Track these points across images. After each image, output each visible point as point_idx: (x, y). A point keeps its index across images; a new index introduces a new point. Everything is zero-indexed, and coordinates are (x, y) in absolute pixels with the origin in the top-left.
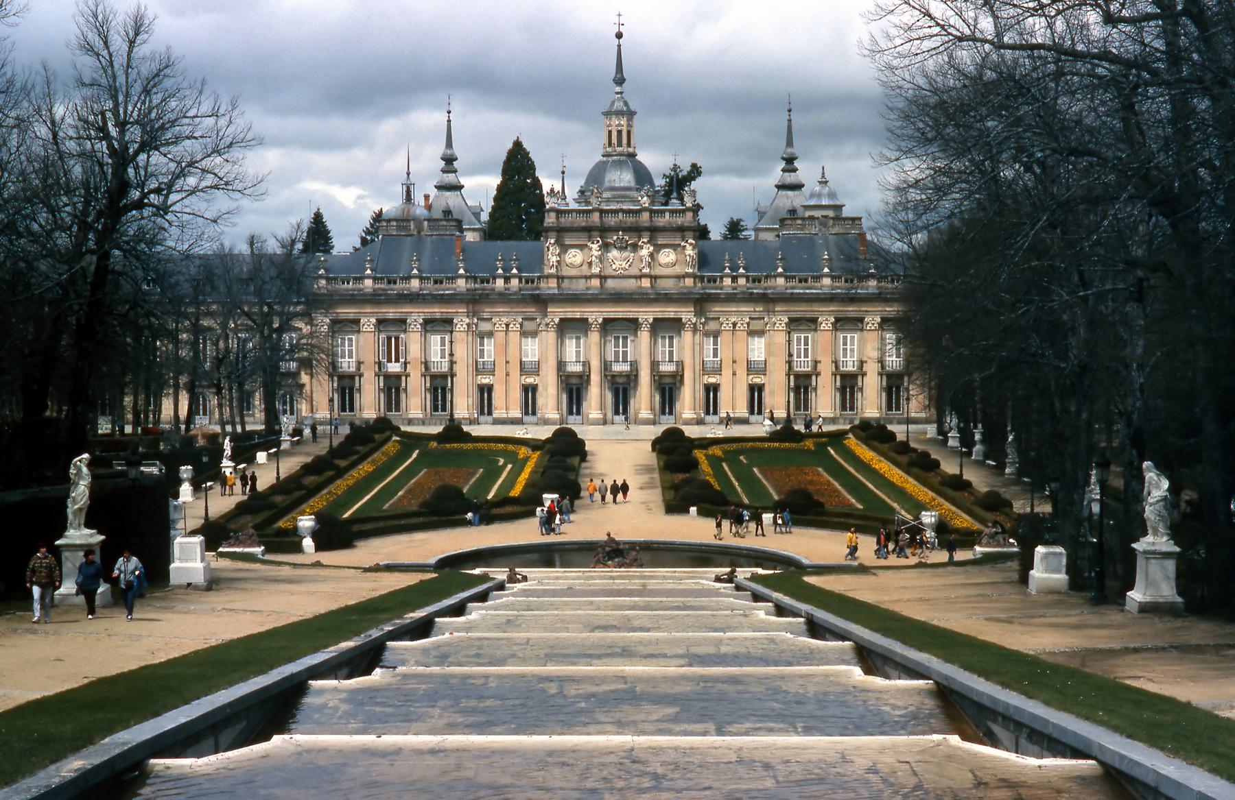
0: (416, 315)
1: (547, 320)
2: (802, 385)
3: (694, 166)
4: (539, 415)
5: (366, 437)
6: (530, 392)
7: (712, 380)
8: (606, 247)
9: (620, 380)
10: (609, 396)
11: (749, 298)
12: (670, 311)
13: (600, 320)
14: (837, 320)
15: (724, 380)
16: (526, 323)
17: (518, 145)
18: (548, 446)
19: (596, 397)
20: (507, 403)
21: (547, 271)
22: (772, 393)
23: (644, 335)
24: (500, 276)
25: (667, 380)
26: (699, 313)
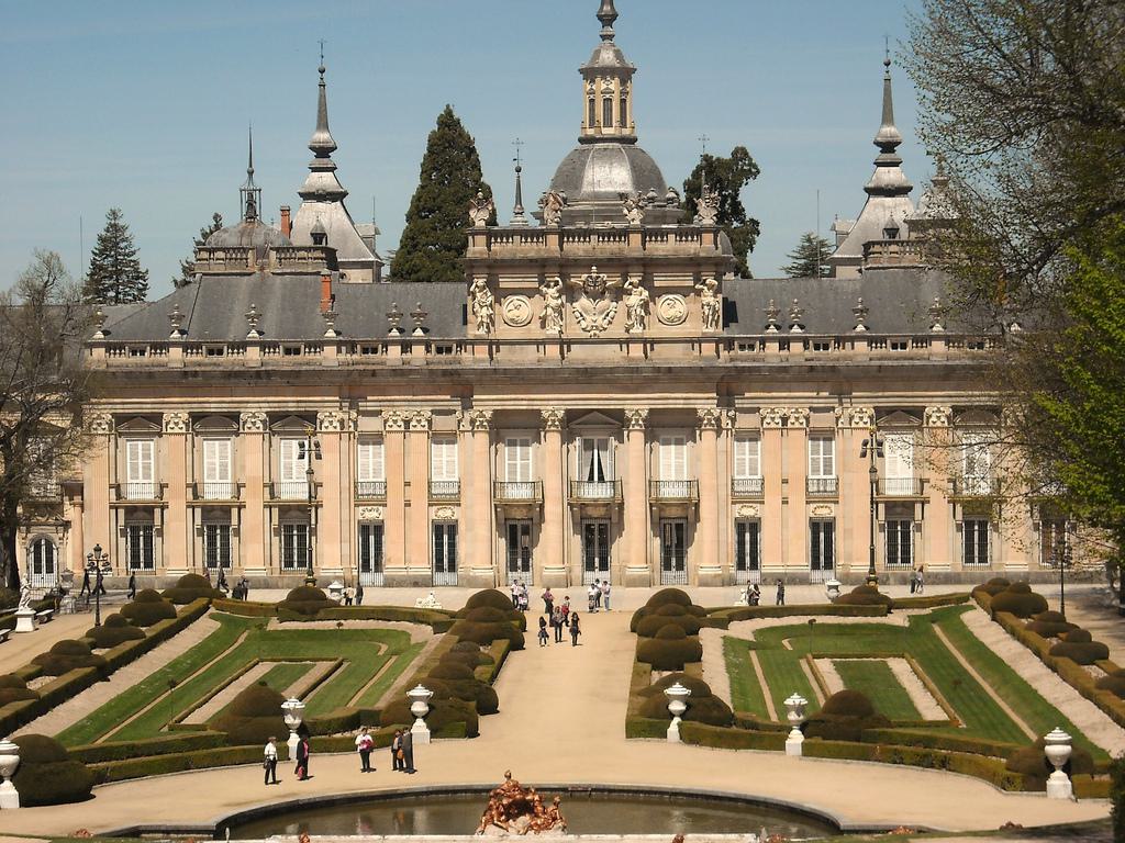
0: (255, 408)
1: (473, 414)
2: (899, 520)
3: (741, 154)
4: (460, 572)
5: (151, 615)
6: (445, 533)
7: (748, 512)
8: (570, 293)
9: (591, 511)
10: (577, 542)
11: (809, 376)
12: (676, 400)
13: (561, 414)
14: (957, 410)
15: (768, 513)
17: (448, 122)
18: (458, 622)
19: (556, 545)
20: (408, 549)
21: (473, 332)
22: (848, 532)
23: (636, 438)
24: (394, 343)
25: (674, 512)
26: (726, 399)
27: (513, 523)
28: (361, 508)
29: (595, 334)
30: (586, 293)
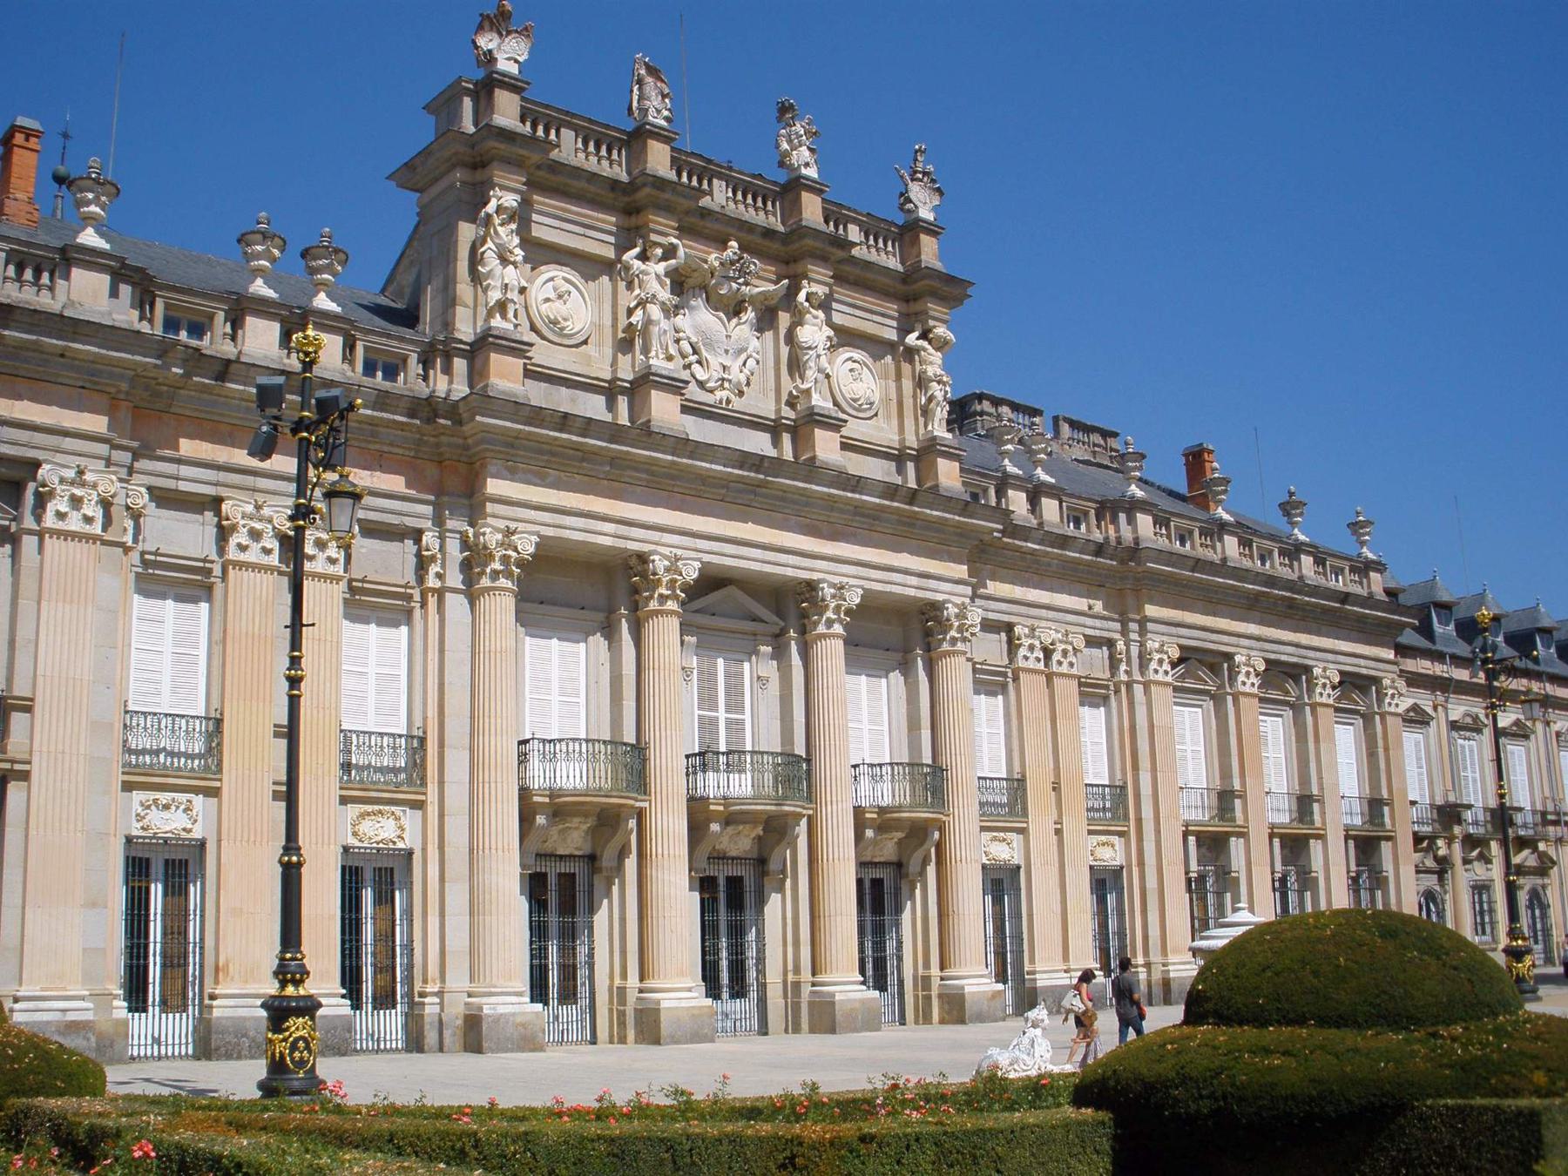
16: (362, 545)
28: (138, 796)
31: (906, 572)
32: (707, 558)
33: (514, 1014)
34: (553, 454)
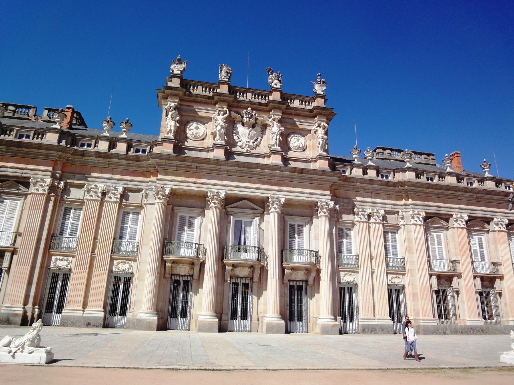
4: (129, 315)
12: (302, 194)
27: (177, 278)
29: (247, 150)
30: (243, 125)
31: (304, 193)
32: (287, 197)
33: (147, 319)
34: (177, 166)
